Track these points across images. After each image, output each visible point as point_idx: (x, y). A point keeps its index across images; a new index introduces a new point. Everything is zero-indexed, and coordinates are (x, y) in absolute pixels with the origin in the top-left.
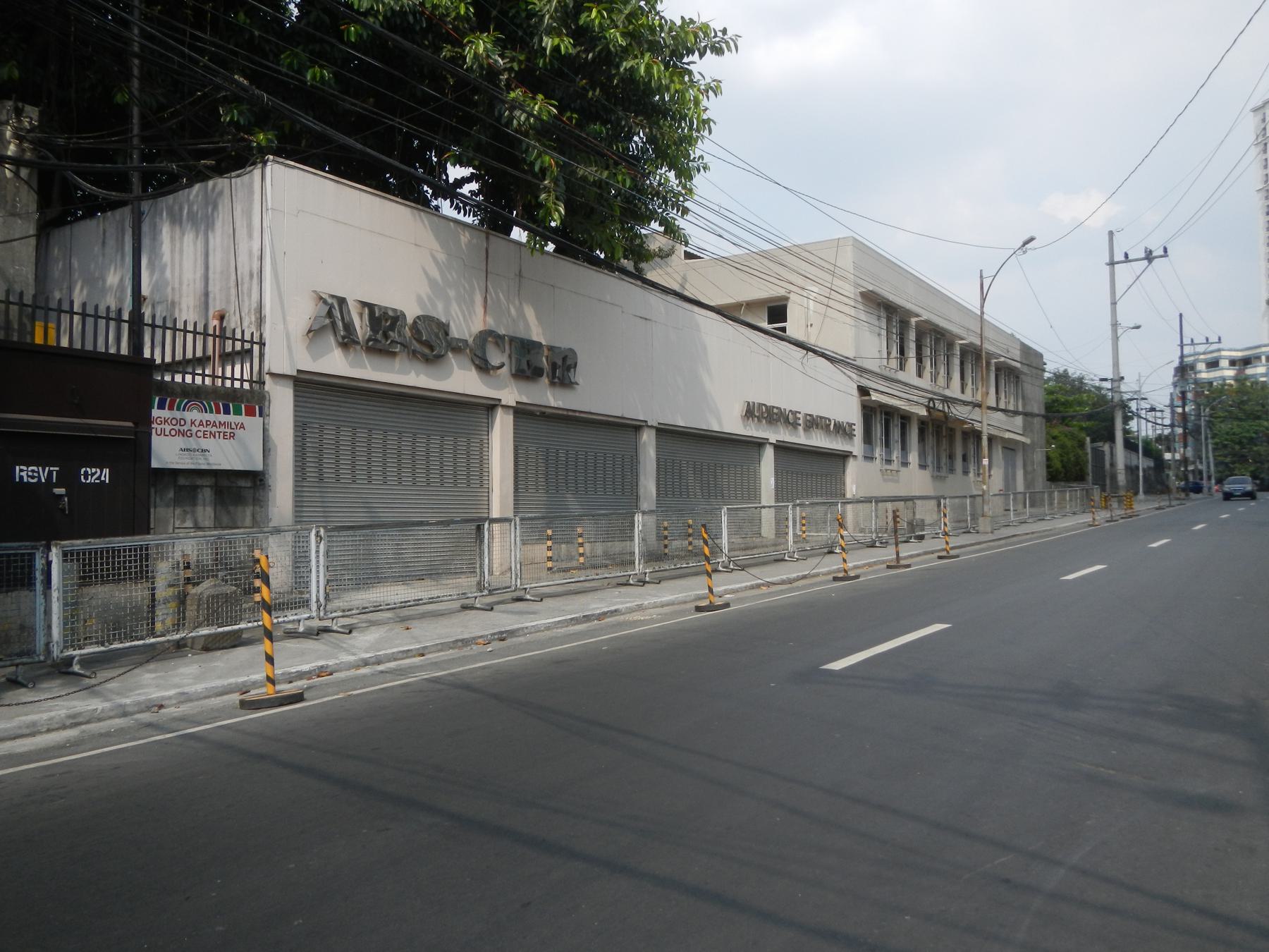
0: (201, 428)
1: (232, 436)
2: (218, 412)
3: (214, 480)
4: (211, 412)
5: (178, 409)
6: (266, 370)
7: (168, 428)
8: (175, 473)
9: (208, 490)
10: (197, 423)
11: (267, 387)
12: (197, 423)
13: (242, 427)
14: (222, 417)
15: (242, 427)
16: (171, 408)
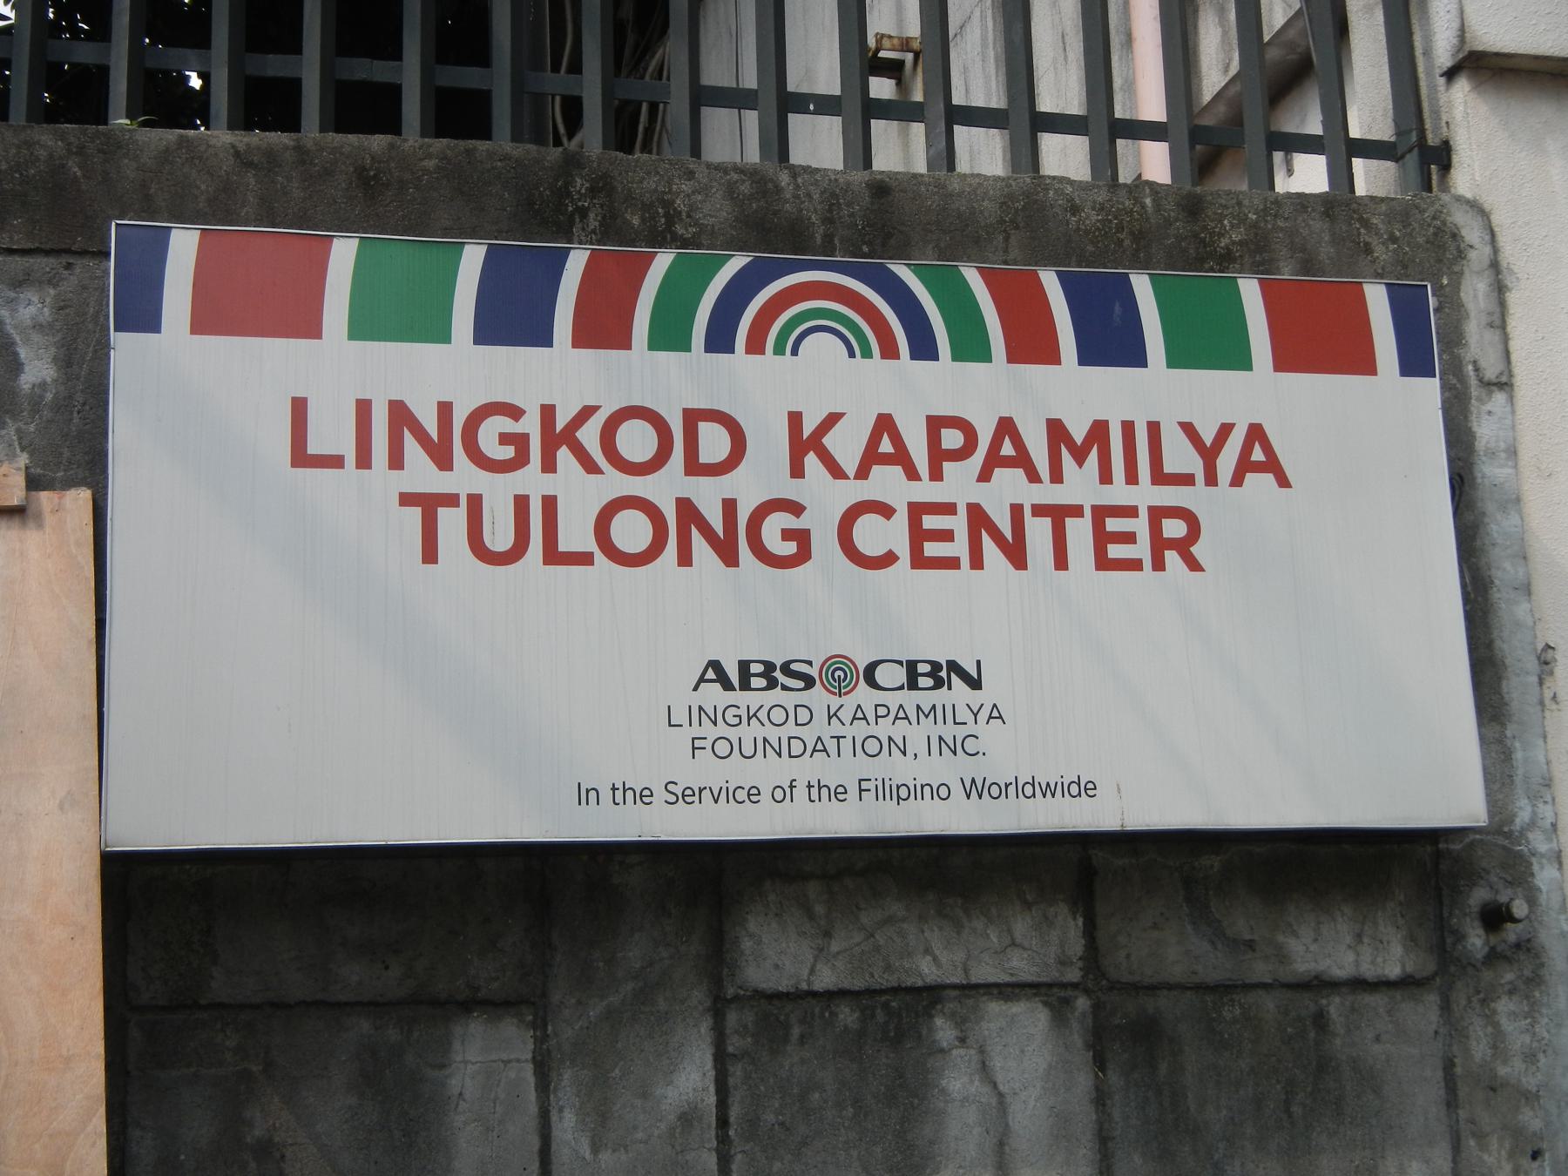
0: (887, 483)
1: (1177, 541)
2: (1032, 345)
3: (1069, 931)
4: (971, 347)
5: (669, 335)
6: (1443, 51)
7: (579, 494)
8: (711, 883)
9: (1032, 1018)
10: (847, 444)
11: (1465, 179)
12: (847, 444)
13: (1260, 457)
14: (1075, 391)
15: (1260, 457)
16: (603, 327)
